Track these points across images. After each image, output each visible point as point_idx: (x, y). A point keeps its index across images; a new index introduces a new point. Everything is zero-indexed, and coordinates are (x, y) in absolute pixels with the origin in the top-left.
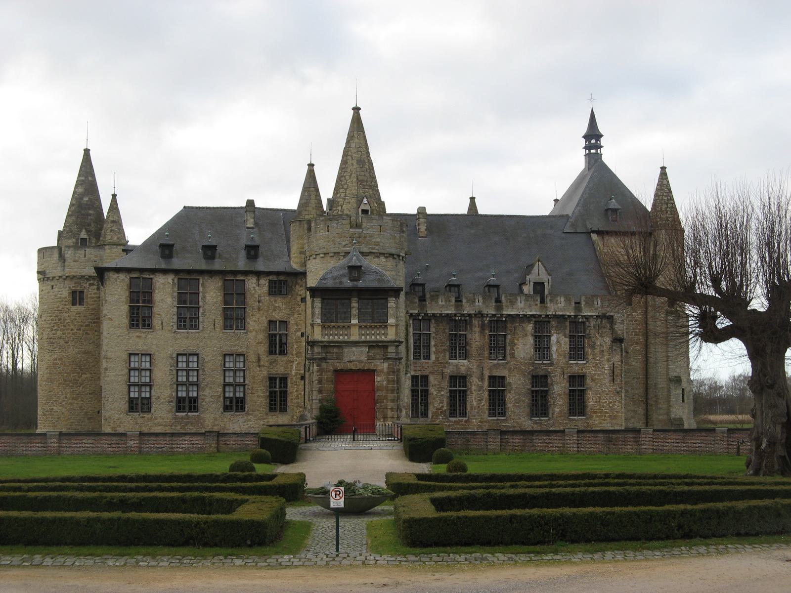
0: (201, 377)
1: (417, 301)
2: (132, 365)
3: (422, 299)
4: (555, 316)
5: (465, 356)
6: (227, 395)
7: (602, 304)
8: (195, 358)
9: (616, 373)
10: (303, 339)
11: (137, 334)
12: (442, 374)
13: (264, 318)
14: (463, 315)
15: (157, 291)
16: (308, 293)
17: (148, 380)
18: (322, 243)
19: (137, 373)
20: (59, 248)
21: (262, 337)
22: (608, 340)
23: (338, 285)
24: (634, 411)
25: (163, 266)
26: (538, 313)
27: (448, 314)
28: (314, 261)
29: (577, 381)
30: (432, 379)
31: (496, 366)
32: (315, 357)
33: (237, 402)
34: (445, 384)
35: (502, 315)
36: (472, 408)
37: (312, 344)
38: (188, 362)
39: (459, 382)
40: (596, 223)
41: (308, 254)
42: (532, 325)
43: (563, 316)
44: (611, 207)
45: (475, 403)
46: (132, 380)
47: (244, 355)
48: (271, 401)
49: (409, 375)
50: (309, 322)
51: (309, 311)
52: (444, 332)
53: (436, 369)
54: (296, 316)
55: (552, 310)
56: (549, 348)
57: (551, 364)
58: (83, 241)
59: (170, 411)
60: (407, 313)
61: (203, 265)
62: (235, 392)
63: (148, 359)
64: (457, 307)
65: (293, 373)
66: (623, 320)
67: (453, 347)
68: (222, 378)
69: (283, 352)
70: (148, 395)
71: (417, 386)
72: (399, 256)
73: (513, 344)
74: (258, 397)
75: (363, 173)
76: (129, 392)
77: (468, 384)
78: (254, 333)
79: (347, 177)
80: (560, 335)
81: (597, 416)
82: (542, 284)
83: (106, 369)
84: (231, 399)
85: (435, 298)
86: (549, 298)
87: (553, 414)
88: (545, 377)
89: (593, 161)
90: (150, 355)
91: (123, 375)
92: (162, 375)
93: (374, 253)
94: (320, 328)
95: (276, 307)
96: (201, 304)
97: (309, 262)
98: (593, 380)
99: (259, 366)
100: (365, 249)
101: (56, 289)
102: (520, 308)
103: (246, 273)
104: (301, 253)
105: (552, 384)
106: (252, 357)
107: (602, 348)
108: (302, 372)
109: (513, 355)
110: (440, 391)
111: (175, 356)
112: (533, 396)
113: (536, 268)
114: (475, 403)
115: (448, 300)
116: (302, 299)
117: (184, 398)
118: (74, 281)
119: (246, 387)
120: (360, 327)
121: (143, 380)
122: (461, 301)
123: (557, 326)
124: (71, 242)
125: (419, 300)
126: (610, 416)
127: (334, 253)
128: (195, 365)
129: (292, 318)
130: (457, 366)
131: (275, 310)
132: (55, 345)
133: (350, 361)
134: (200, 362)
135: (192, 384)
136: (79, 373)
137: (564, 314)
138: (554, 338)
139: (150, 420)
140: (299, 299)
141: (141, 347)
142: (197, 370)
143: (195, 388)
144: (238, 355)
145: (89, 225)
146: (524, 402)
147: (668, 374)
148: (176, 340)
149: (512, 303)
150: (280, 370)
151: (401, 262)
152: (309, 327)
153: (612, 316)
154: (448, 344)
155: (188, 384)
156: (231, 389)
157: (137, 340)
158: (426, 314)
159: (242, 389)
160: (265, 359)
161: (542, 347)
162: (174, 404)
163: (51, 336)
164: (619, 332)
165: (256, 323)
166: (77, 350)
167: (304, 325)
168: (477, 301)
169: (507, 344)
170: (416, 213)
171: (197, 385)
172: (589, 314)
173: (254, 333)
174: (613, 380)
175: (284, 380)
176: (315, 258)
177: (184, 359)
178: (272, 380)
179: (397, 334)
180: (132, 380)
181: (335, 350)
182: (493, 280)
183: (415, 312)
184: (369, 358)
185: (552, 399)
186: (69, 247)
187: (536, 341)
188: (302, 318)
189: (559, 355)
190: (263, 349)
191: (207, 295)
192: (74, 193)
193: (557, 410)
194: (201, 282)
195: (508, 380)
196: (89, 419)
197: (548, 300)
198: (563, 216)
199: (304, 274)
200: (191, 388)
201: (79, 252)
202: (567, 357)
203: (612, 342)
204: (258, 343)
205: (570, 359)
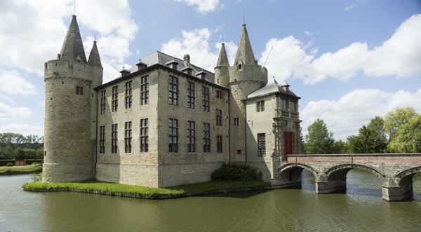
21: (215, 116)
74: (214, 146)
92: (183, 131)
141: (174, 116)
162: (187, 148)
165: (213, 109)
190: (215, 122)
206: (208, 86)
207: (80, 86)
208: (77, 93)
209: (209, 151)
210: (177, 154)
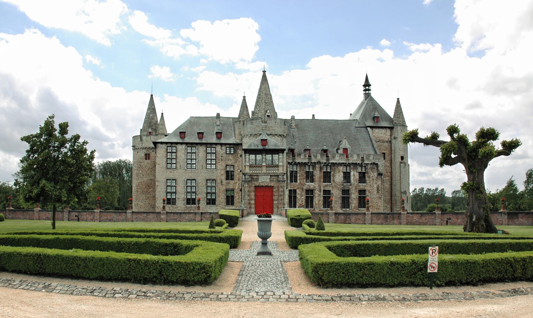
0: (197, 190)
1: (291, 156)
2: (168, 184)
3: (294, 155)
4: (353, 164)
5: (312, 181)
6: (208, 197)
7: (373, 158)
8: (194, 181)
9: (379, 189)
10: (241, 173)
11: (170, 171)
12: (302, 189)
13: (224, 164)
14: (312, 163)
15: (178, 152)
16: (243, 151)
17: (174, 191)
18: (249, 130)
19: (170, 188)
20: (141, 136)
21: (223, 172)
22: (376, 174)
23: (256, 148)
24: (386, 207)
25: (181, 141)
26: (345, 162)
27: (305, 162)
28: (246, 138)
29: (362, 192)
30: (298, 191)
31: (327, 186)
32: (246, 180)
33: (212, 201)
34: (304, 193)
35: (329, 163)
36: (316, 204)
37: (244, 174)
38: (191, 183)
39: (310, 192)
40: (370, 123)
41: (243, 135)
42: (342, 167)
43: (356, 163)
44: (376, 116)
45: (317, 202)
46: (168, 191)
47: (215, 180)
48: (227, 200)
49: (288, 189)
50: (244, 164)
51: (244, 161)
52: (304, 170)
53: (300, 187)
54: (238, 163)
55: (351, 161)
56: (349, 177)
57: (351, 185)
58: (150, 133)
59: (184, 204)
60: (287, 161)
61: (198, 141)
62: (211, 196)
63: (175, 181)
64: (309, 159)
65: (237, 188)
66: (382, 165)
67: (307, 178)
68: (206, 190)
69: (232, 179)
70: (174, 197)
71: (292, 194)
72: (283, 136)
73: (334, 176)
74: (221, 198)
75: (267, 99)
76: (167, 196)
77: (314, 193)
78: (220, 170)
79: (260, 101)
80: (355, 172)
81: (371, 208)
82: (347, 149)
83: (157, 186)
84: (209, 199)
85: (299, 155)
86: (350, 155)
87: (351, 207)
88: (348, 191)
89: (367, 96)
90: (175, 180)
91: (164, 188)
92: (181, 189)
93: (272, 134)
94: (249, 167)
95: (229, 159)
96: (197, 158)
97: (243, 139)
98: (369, 192)
99: (222, 185)
100: (269, 133)
101: (139, 153)
102: (337, 159)
103: (216, 144)
104: (240, 135)
105: (351, 194)
106: (219, 181)
107: (373, 178)
108: (241, 187)
109: (334, 181)
110: (301, 197)
111: (186, 180)
112: (343, 199)
113: (344, 142)
114: (317, 202)
115: (305, 156)
116: (240, 155)
117: (190, 199)
118: (146, 149)
119: (216, 194)
120: (267, 167)
121: (173, 191)
122: (311, 157)
123: (353, 168)
124: (145, 133)
125: (292, 156)
126: (376, 208)
127: (255, 134)
128: (194, 184)
129: (236, 164)
130: (309, 185)
131: (228, 160)
132: (139, 177)
133: (262, 182)
134: (197, 183)
135: (193, 192)
136: (148, 188)
137: (356, 162)
138: (352, 173)
139: (176, 208)
140: (239, 155)
141: (171, 176)
142: (195, 187)
143: (194, 194)
144: (213, 180)
145: (152, 126)
146: (339, 201)
147: (401, 190)
148: (186, 173)
149: (334, 157)
150: (231, 187)
151: (285, 139)
152: (244, 167)
153: (377, 164)
154: (305, 176)
155: (192, 192)
156: (210, 195)
157: (170, 173)
158: (295, 162)
159: (214, 195)
160: (224, 181)
161: (347, 176)
162: (185, 201)
163: (137, 173)
164: (381, 171)
166: (147, 179)
167: (241, 167)
168: (318, 156)
169: (331, 176)
170: (290, 119)
171: (195, 193)
172: (368, 162)
173: (220, 170)
174: (378, 192)
175: (233, 190)
176: (246, 137)
177: (190, 181)
178: (227, 190)
179: (283, 170)
180: (168, 191)
181: (255, 177)
182: (325, 148)
183: (291, 161)
184: (270, 181)
185: (351, 200)
186: (144, 135)
187: (344, 175)
188: (241, 164)
189: (354, 181)
190: (224, 177)
191: (199, 154)
192: (147, 113)
193: (353, 205)
194: (197, 148)
195: (332, 192)
196: (152, 208)
197: (349, 156)
198: (354, 120)
199: (241, 144)
200: (193, 194)
201: (148, 137)
202: (358, 182)
203: (378, 175)
204: (221, 175)
205: (359, 183)
206: (214, 146)
207: (148, 153)
208: (146, 159)
209: (215, 205)
210: (174, 206)
